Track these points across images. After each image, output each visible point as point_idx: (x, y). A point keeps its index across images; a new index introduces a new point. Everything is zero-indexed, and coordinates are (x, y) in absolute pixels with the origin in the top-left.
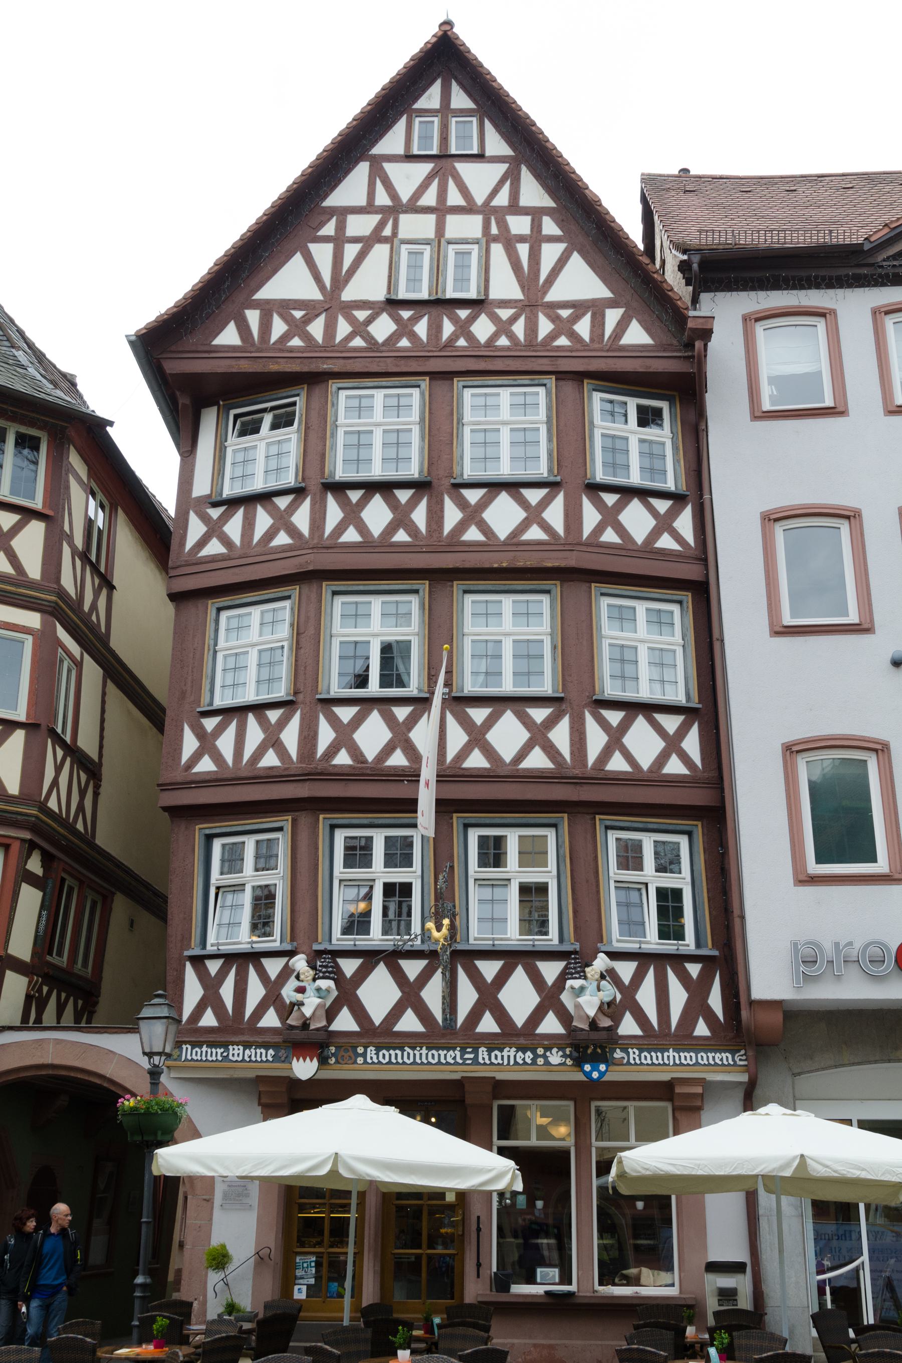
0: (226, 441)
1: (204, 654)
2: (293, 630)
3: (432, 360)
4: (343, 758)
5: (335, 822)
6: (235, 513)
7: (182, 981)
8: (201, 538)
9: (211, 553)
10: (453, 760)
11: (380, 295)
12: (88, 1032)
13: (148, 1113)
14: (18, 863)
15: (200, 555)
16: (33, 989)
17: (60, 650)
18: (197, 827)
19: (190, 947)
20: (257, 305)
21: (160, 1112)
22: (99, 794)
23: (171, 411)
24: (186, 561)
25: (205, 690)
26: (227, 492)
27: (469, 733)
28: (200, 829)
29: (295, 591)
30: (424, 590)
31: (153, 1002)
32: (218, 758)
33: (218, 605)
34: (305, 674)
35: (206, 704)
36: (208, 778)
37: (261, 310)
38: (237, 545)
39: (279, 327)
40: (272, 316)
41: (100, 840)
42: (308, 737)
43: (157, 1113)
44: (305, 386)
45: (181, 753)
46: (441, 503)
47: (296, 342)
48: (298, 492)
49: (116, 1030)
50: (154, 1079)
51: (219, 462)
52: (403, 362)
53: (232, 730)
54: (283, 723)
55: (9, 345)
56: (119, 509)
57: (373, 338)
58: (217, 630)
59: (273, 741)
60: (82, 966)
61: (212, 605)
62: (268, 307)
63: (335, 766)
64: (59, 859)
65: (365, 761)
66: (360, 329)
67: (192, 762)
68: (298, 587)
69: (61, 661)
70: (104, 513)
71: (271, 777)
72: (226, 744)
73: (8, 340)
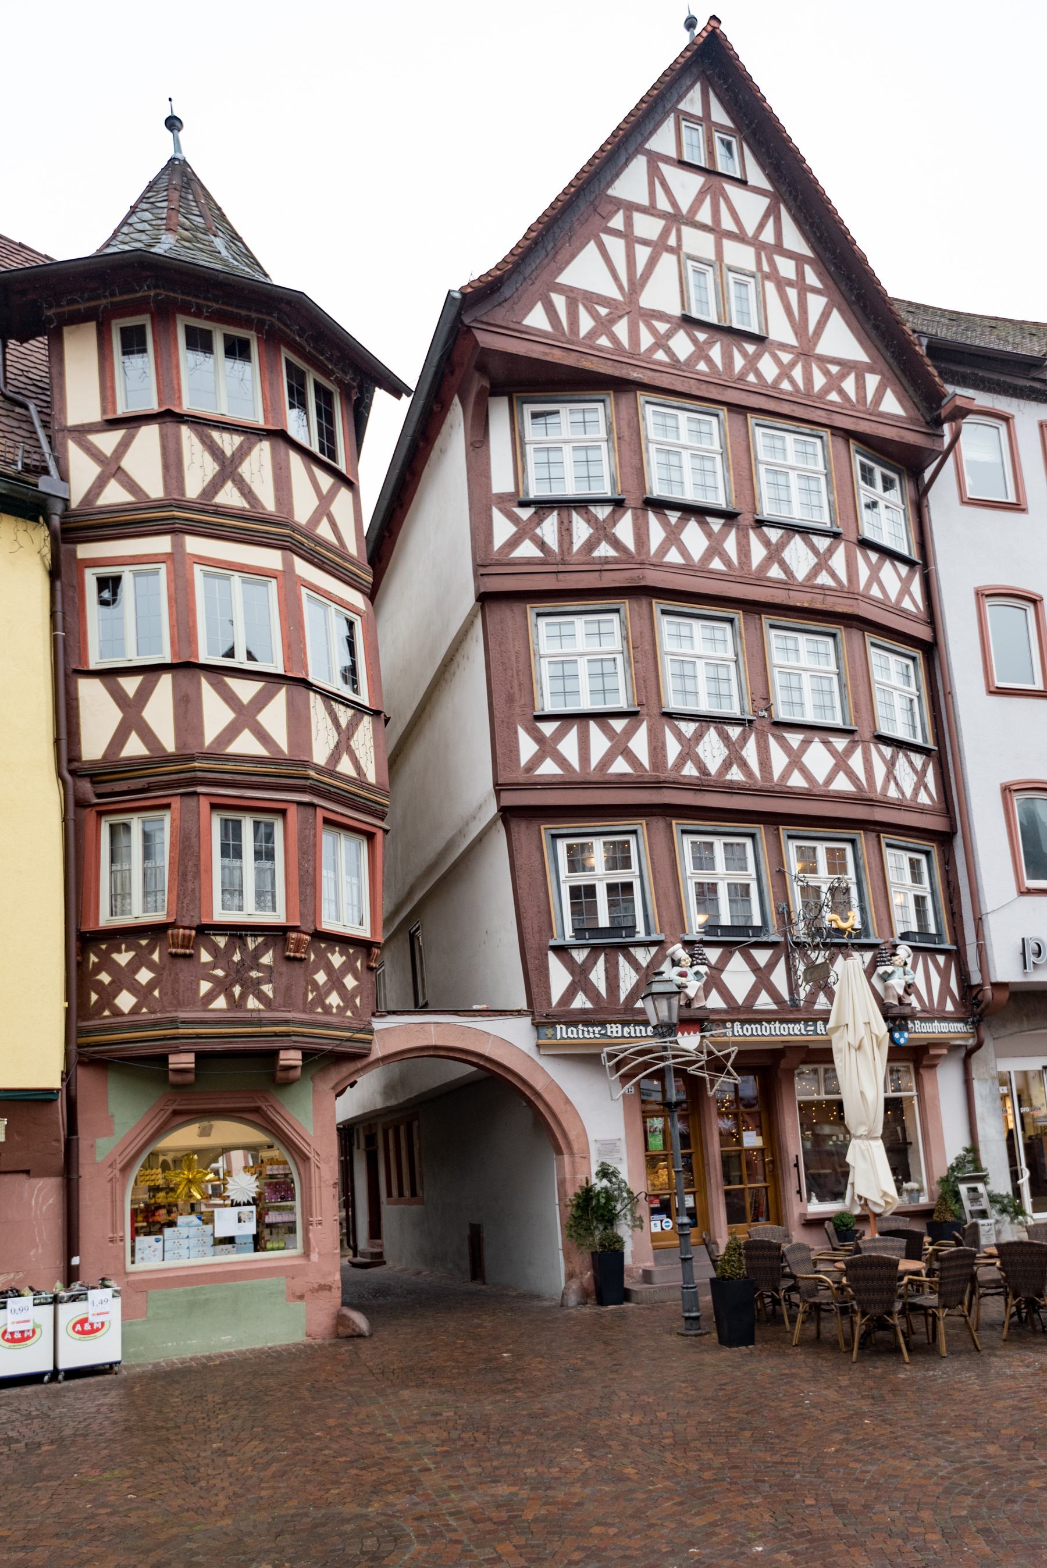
2: (628, 643)
3: (730, 390)
4: (690, 770)
5: (685, 827)
10: (779, 779)
11: (675, 310)
27: (789, 756)
29: (625, 605)
30: (739, 619)
32: (561, 761)
34: (646, 687)
42: (657, 748)
46: (747, 536)
48: (618, 504)
52: (704, 386)
53: (574, 733)
54: (629, 733)
57: (674, 355)
59: (620, 747)
63: (685, 776)
65: (709, 774)
66: (661, 342)
68: (627, 601)
71: (621, 783)
72: (569, 747)
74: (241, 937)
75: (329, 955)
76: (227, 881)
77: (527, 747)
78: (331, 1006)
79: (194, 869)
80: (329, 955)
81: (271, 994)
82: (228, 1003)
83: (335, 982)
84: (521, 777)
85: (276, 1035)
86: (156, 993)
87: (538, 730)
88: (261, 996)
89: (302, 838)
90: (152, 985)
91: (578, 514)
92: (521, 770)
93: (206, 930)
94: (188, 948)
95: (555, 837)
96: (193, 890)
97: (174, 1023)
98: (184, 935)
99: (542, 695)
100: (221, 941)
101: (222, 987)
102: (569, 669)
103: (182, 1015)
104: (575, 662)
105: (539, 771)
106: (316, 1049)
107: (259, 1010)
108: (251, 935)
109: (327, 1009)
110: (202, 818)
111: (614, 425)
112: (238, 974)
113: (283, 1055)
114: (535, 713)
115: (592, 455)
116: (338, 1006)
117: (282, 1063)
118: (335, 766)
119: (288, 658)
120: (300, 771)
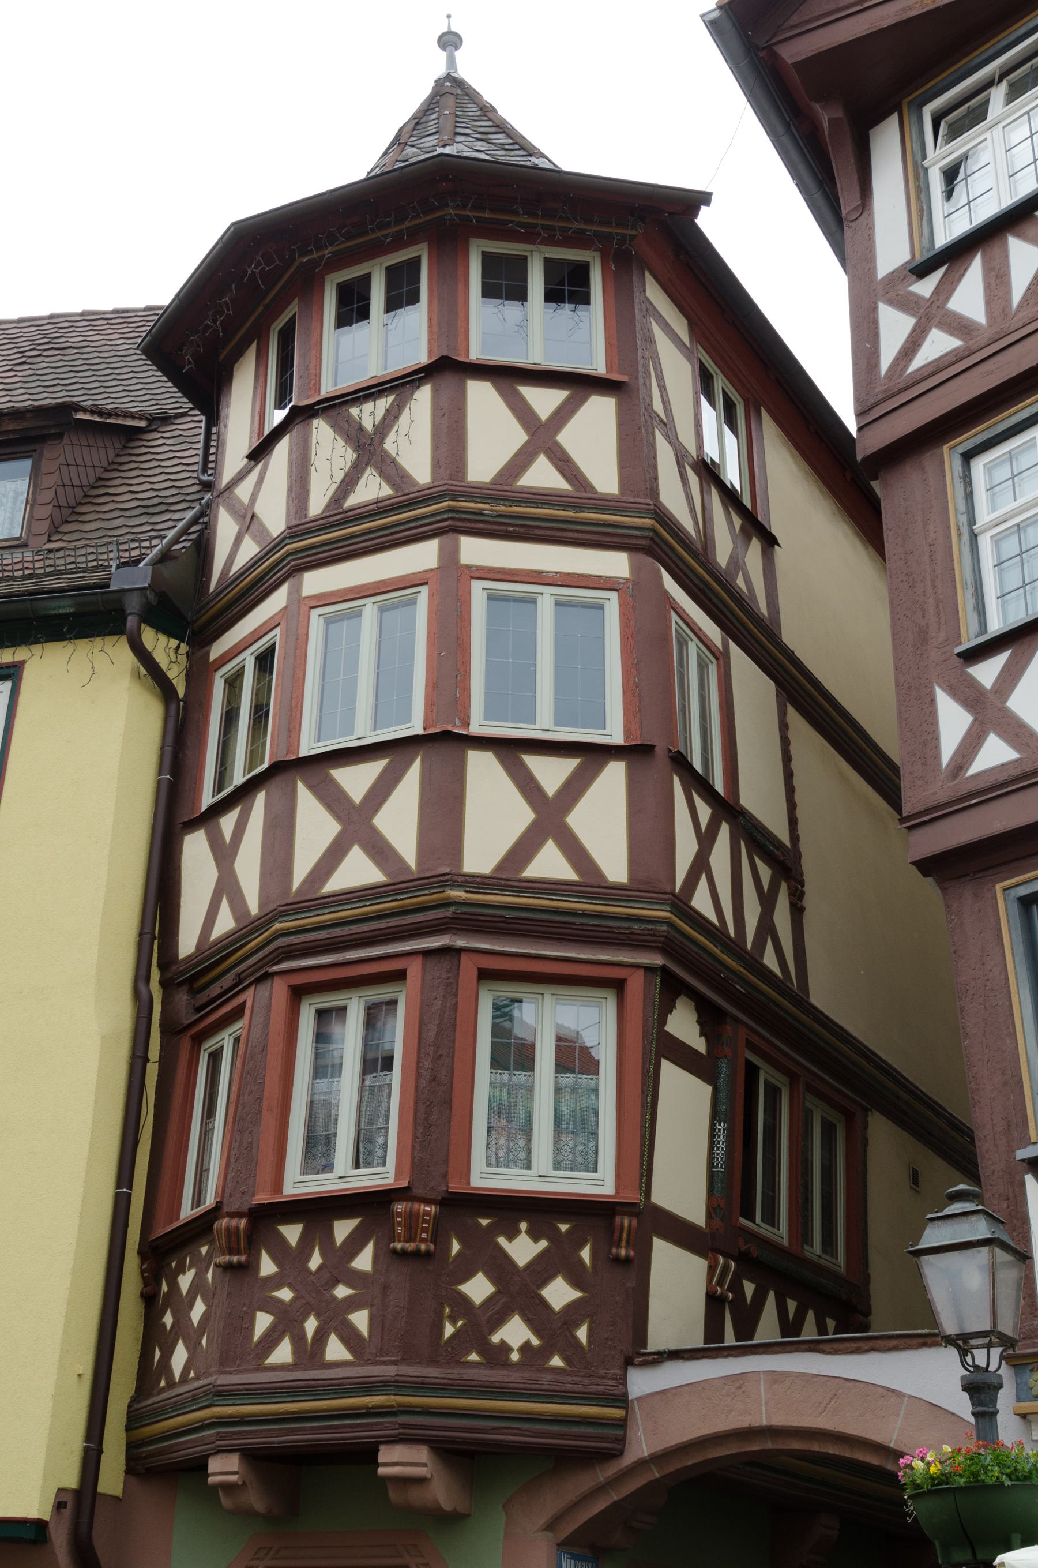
0: (924, 157)
1: (951, 547)
6: (966, 270)
8: (907, 341)
9: (931, 359)
12: (836, 1352)
13: (977, 1488)
14: (644, 1016)
15: (910, 370)
16: (720, 1283)
17: (674, 617)
18: (998, 887)
21: (1008, 1483)
22: (802, 910)
23: (820, 184)
24: (885, 391)
25: (965, 610)
26: (942, 239)
28: (1005, 889)
31: (947, 1211)
33: (961, 449)
35: (972, 633)
36: (1003, 777)
38: (979, 324)
41: (818, 998)
43: (999, 1486)
45: (937, 747)
49: (894, 1342)
50: (981, 1404)
51: (919, 199)
55: (525, 153)
56: (764, 414)
58: (969, 496)
60: (824, 1251)
61: (950, 455)
64: (737, 1020)
67: (964, 756)
69: (682, 644)
70: (737, 436)
73: (522, 148)
78: (505, 1348)
80: (502, 1241)
91: (1019, 236)
105: (974, 769)
113: (386, 1454)
117: (381, 1471)
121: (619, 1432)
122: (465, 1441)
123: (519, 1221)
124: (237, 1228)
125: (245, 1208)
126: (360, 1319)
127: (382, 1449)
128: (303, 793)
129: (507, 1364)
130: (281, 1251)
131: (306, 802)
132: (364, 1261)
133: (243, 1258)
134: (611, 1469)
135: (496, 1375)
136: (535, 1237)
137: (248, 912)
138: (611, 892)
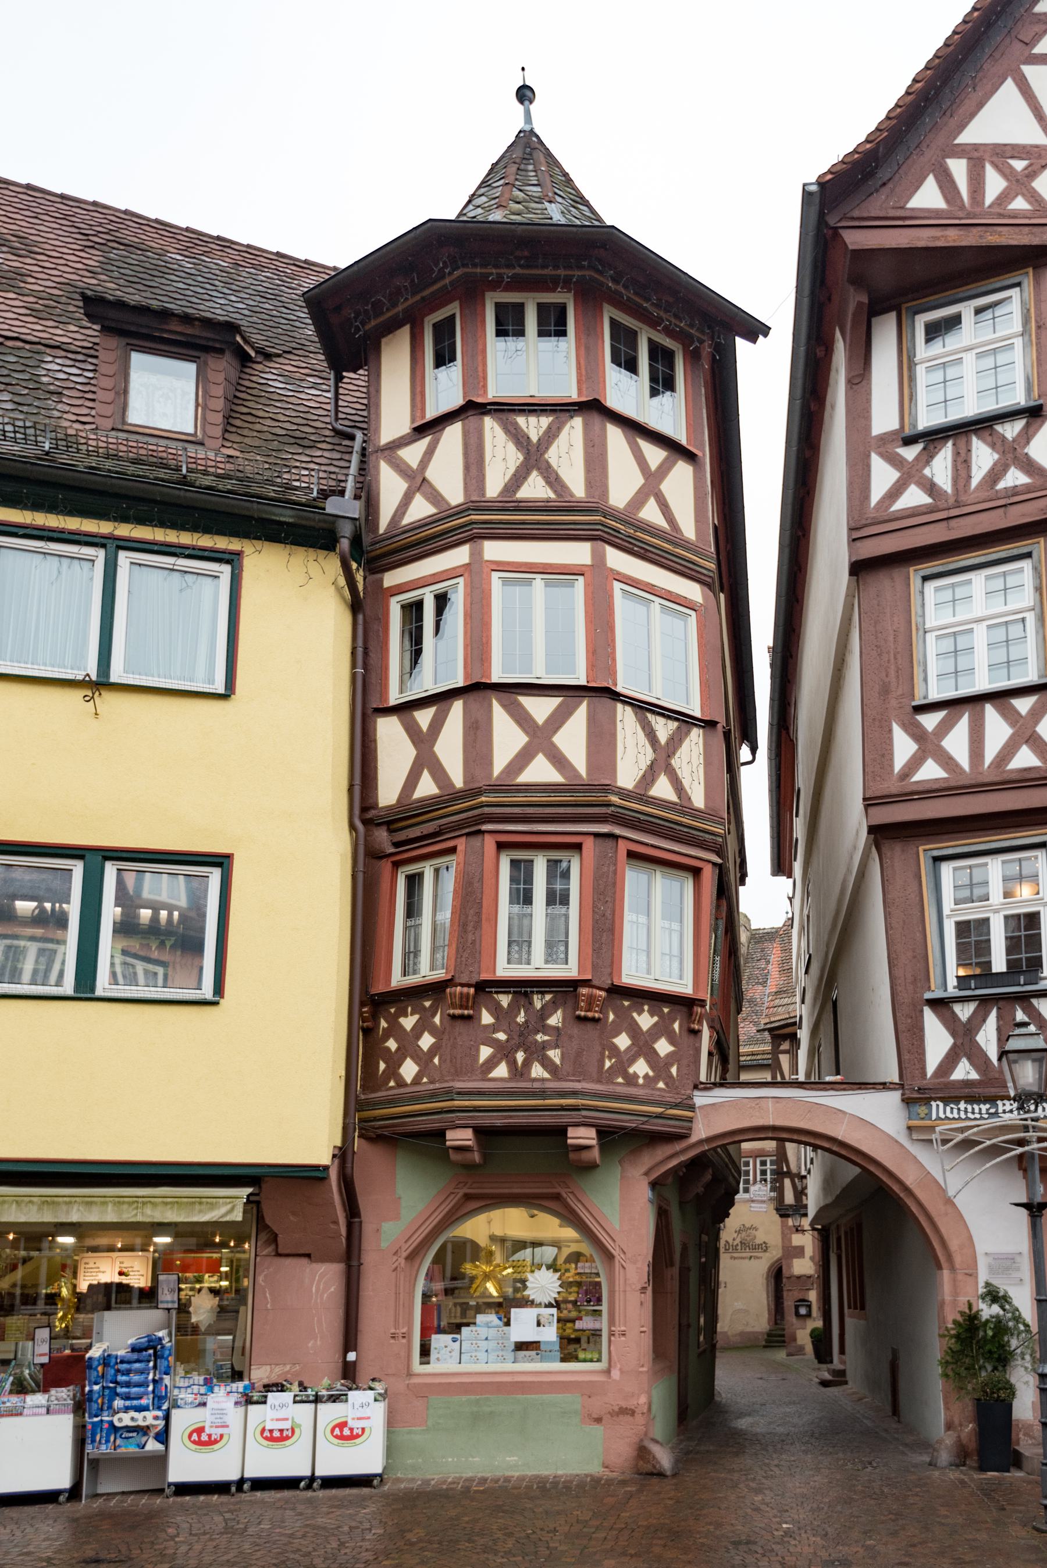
7: (922, 1029)
19: (929, 989)
20: (961, 151)
32: (947, 761)
37: (969, 159)
39: (994, 184)
40: (983, 167)
44: (1030, 270)
47: (1020, 204)
53: (963, 725)
62: (976, 155)
74: (526, 994)
75: (635, 1015)
76: (515, 930)
77: (903, 747)
79: (475, 918)
80: (635, 1015)
81: (557, 1061)
82: (509, 1071)
83: (643, 1046)
84: (893, 787)
85: (563, 1108)
86: (436, 1061)
87: (919, 725)
88: (546, 1063)
89: (598, 877)
90: (434, 1050)
92: (895, 778)
93: (486, 988)
94: (467, 1008)
95: (938, 860)
96: (473, 942)
97: (449, 1094)
98: (461, 994)
99: (925, 680)
100: (505, 1000)
101: (504, 1052)
102: (962, 642)
103: (459, 1085)
104: (971, 630)
105: (918, 777)
106: (615, 1127)
107: (543, 1080)
108: (538, 992)
109: (631, 1080)
110: (485, 859)
111: (1032, 310)
112: (522, 1038)
113: (571, 1132)
114: (914, 704)
115: (1002, 358)
116: (646, 1076)
117: (569, 1141)
118: (646, 790)
119: (591, 666)
120: (600, 798)
121: (689, 1124)
122: (609, 1126)
123: (643, 1004)
124: (468, 994)
125: (473, 981)
126: (555, 1055)
127: (570, 1129)
128: (498, 711)
129: (636, 1085)
130: (496, 1010)
131: (500, 717)
132: (555, 1020)
133: (471, 1012)
134: (684, 1144)
135: (632, 1091)
136: (652, 1016)
137: (452, 785)
138: (695, 813)
